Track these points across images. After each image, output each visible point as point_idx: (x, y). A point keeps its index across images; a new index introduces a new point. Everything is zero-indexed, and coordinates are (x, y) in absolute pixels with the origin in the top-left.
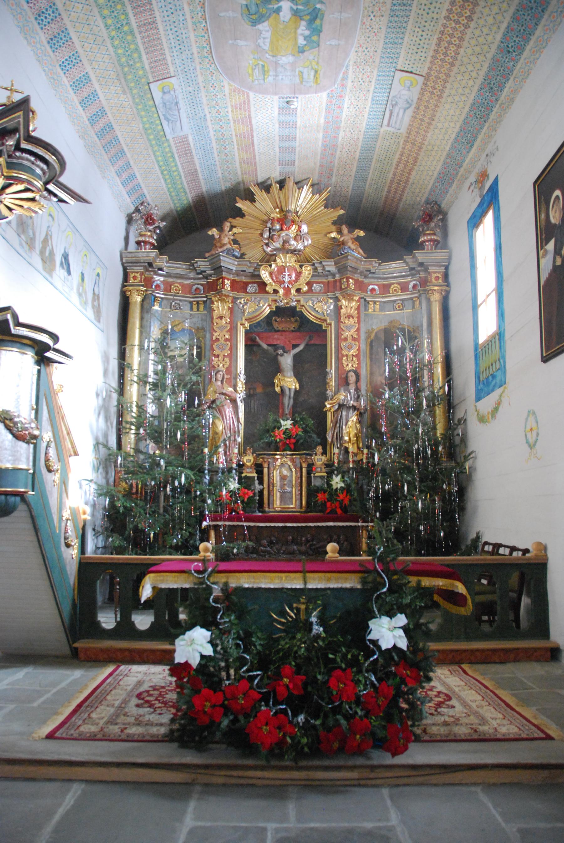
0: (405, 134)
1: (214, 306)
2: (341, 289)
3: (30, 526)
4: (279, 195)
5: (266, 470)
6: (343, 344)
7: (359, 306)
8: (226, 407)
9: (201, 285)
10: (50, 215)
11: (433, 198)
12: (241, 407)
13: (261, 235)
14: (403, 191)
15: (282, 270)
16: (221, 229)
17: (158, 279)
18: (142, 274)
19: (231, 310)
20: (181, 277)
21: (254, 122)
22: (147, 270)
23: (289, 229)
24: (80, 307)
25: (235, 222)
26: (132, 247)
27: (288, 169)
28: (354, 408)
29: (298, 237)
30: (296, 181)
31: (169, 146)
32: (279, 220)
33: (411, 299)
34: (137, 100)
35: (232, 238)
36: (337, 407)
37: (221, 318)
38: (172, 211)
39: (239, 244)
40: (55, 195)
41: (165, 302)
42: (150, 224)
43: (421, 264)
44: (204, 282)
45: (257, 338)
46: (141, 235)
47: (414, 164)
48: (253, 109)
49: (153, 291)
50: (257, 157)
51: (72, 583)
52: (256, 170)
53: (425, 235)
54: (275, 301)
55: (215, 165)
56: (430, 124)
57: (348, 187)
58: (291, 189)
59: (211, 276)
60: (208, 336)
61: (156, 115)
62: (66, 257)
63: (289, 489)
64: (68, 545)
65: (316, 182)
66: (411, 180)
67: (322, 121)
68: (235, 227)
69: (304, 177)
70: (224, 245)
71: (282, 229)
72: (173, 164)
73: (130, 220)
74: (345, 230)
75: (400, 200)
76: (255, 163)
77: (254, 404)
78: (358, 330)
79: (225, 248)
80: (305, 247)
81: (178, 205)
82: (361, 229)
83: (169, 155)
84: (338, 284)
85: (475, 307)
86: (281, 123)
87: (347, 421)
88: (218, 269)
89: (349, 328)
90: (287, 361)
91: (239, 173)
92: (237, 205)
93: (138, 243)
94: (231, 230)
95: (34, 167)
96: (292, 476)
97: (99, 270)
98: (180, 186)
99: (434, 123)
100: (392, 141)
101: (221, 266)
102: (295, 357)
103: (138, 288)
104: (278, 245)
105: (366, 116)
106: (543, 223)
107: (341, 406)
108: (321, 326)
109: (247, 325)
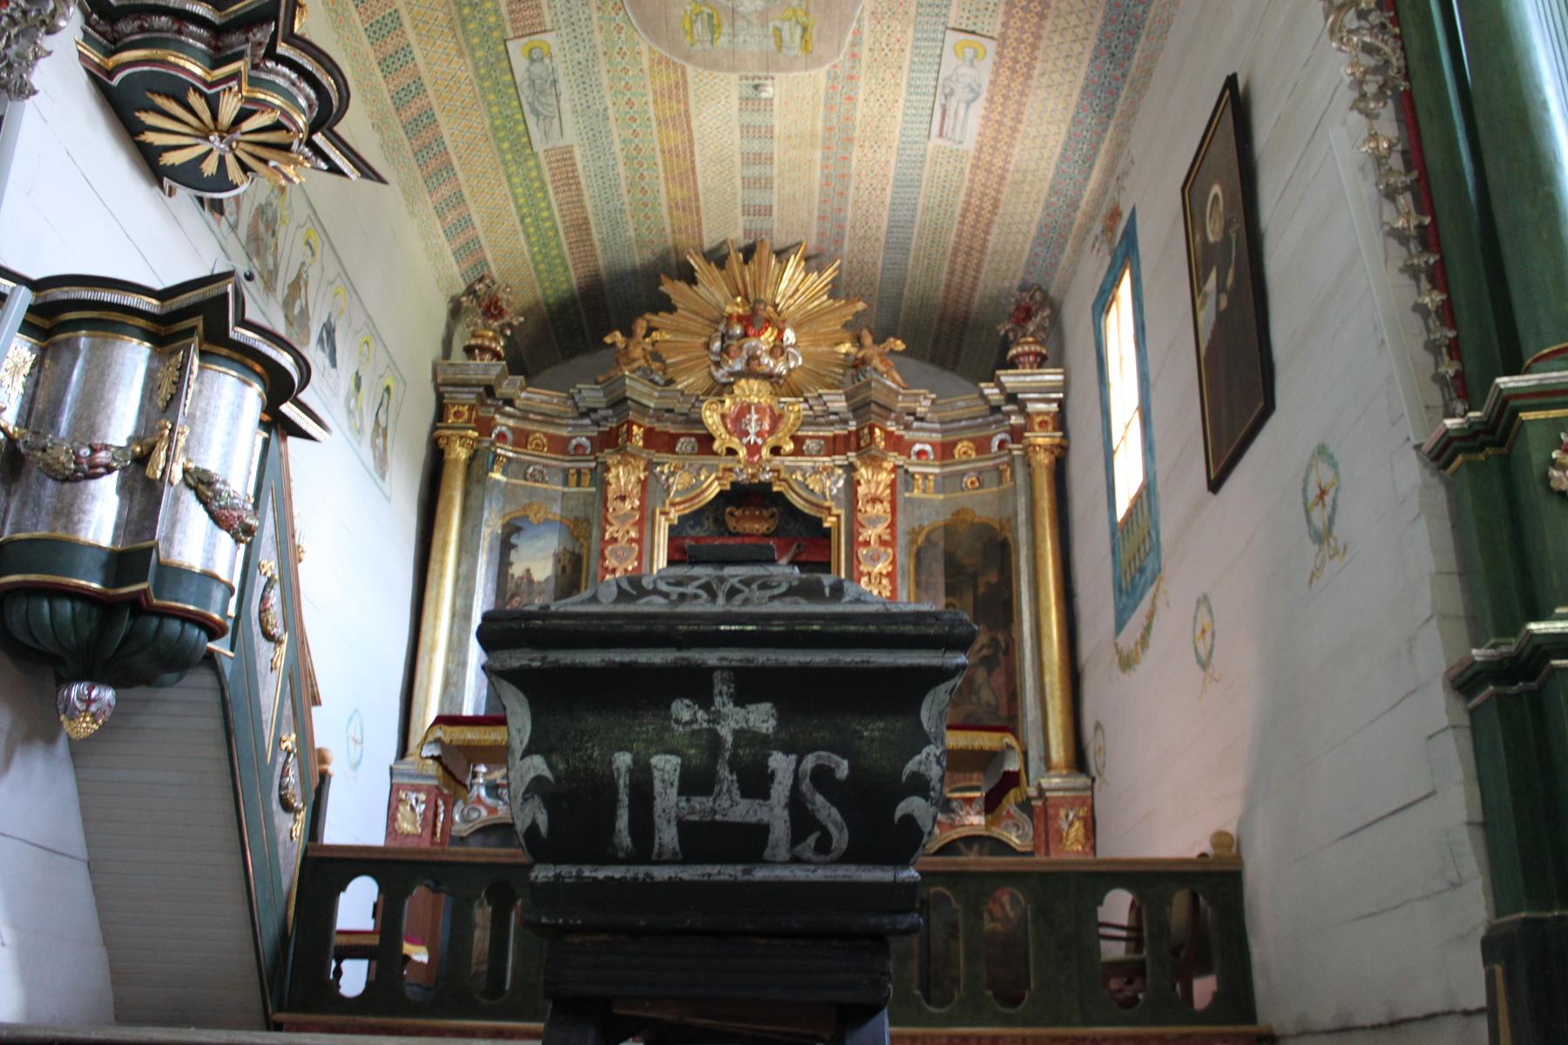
0: (972, 153)
1: (611, 477)
2: (858, 448)
3: (216, 724)
4: (742, 273)
6: (863, 552)
10: (308, 243)
11: (1033, 279)
13: (707, 346)
14: (979, 265)
16: (628, 333)
17: (503, 424)
18: (471, 408)
19: (643, 484)
21: (694, 124)
22: (483, 404)
23: (758, 335)
24: (348, 434)
25: (656, 319)
26: (458, 356)
27: (759, 223)
29: (778, 350)
30: (777, 247)
31: (538, 167)
32: (740, 319)
33: (996, 468)
34: (482, 71)
35: (649, 348)
37: (623, 498)
38: (537, 303)
39: (663, 362)
40: (326, 158)
41: (513, 466)
42: (495, 317)
43: (1011, 398)
46: (474, 335)
47: (993, 213)
48: (692, 99)
49: (493, 443)
50: (701, 197)
51: (285, 888)
52: (700, 224)
55: (622, 211)
56: (1014, 130)
57: (874, 264)
59: (606, 419)
60: (595, 533)
61: (515, 103)
62: (329, 331)
64: (287, 806)
65: (813, 252)
66: (990, 245)
67: (820, 126)
68: (656, 329)
69: (791, 241)
70: (634, 360)
71: (745, 335)
72: (543, 205)
73: (456, 311)
74: (868, 340)
75: (973, 289)
76: (698, 209)
78: (892, 526)
79: (636, 365)
80: (790, 370)
81: (549, 292)
82: (897, 337)
83: (537, 185)
84: (853, 439)
86: (745, 128)
88: (619, 403)
89: (874, 521)
91: (668, 230)
93: (469, 350)
94: (648, 334)
95: (294, 90)
97: (389, 381)
98: (554, 252)
99: (1021, 127)
100: (950, 168)
101: (626, 399)
103: (463, 433)
104: (739, 366)
105: (899, 116)
106: (1199, 248)
108: (820, 521)
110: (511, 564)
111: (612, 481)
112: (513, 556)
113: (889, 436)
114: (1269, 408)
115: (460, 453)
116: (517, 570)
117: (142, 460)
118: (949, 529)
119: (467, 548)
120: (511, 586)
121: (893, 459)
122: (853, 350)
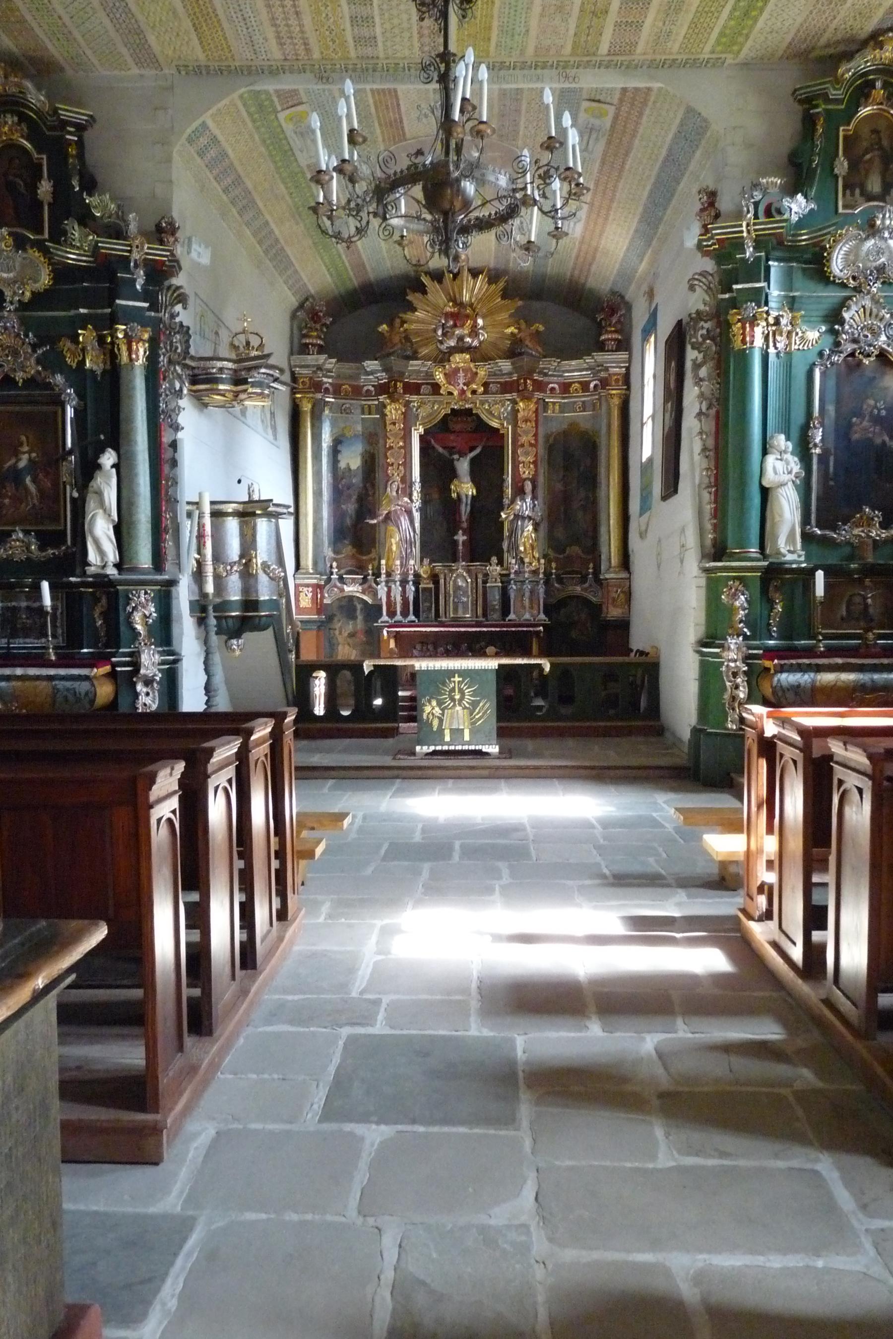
1: (387, 411)
2: (519, 391)
5: (442, 581)
7: (537, 409)
8: (402, 519)
9: (373, 386)
12: (417, 516)
13: (435, 331)
15: (457, 370)
28: (530, 518)
36: (512, 517)
37: (394, 424)
39: (411, 342)
45: (433, 441)
53: (608, 332)
55: (384, 259)
58: (465, 278)
60: (381, 441)
63: (465, 599)
68: (406, 322)
71: (455, 326)
74: (523, 326)
77: (430, 510)
78: (536, 435)
80: (481, 343)
85: (642, 425)
87: (523, 531)
89: (526, 433)
90: (463, 466)
92: (407, 298)
94: (402, 326)
96: (467, 586)
104: (452, 343)
107: (517, 517)
109: (421, 430)
110: (338, 461)
111: (388, 413)
112: (340, 457)
114: (676, 491)
115: (306, 407)
116: (342, 465)
117: (248, 565)
118: (565, 434)
120: (340, 473)
121: (538, 395)
122: (516, 331)
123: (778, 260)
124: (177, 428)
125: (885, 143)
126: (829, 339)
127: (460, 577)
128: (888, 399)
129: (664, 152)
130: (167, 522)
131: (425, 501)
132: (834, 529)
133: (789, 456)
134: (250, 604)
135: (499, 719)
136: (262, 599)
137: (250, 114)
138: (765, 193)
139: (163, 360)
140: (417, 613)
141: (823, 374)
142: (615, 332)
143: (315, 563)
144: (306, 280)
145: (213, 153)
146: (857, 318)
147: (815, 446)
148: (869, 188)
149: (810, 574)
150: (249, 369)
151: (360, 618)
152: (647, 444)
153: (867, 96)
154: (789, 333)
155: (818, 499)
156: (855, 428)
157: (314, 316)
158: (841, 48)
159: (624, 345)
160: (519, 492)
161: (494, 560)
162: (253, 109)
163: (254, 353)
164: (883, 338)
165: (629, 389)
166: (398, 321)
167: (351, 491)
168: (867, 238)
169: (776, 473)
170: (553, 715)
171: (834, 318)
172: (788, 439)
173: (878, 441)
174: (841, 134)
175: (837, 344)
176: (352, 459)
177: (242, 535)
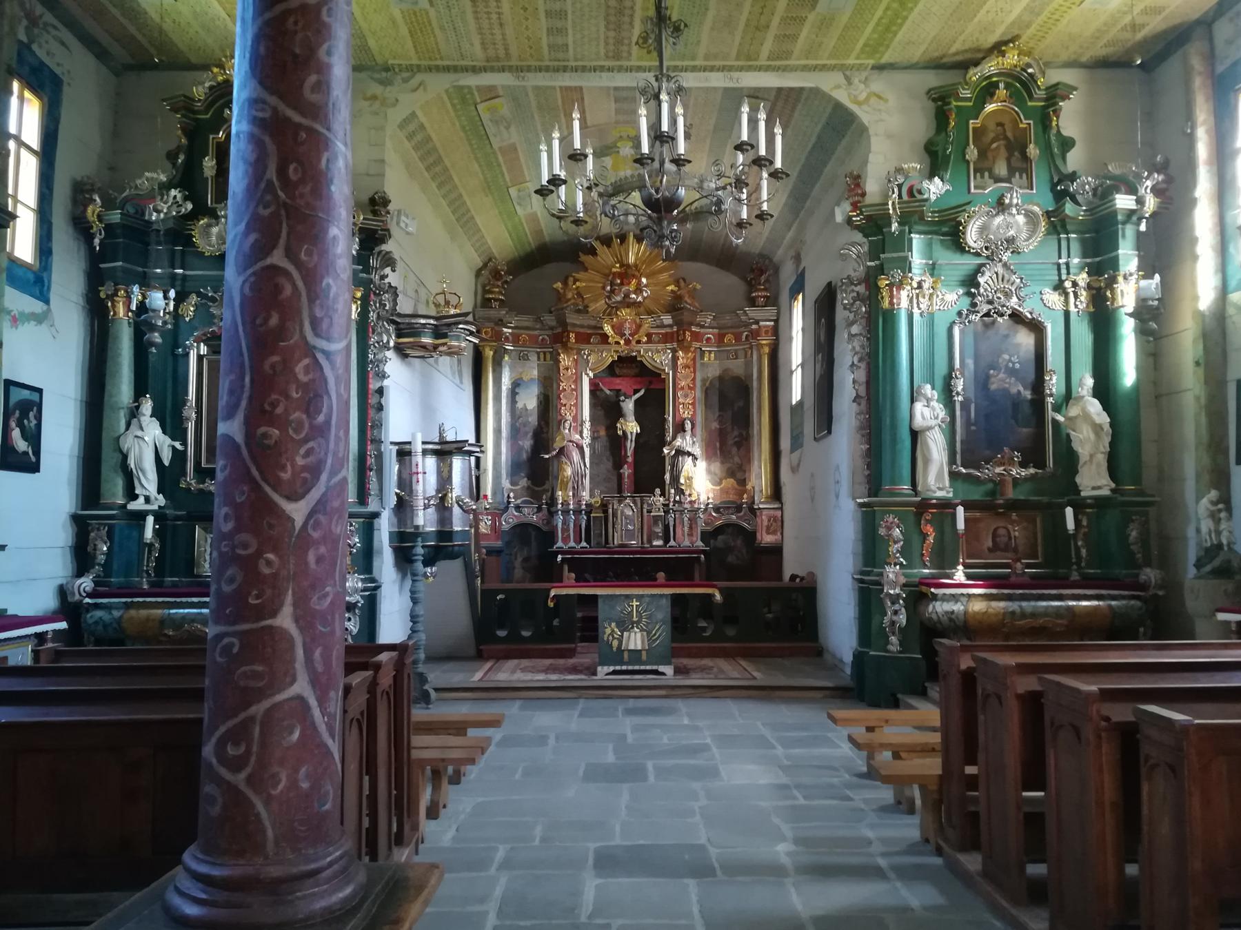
12: (587, 451)
13: (604, 288)
19: (576, 361)
20: (527, 328)
44: (550, 332)
54: (617, 352)
71: (622, 284)
74: (682, 284)
77: (598, 446)
78: (694, 380)
80: (645, 298)
88: (563, 323)
90: (629, 406)
102: (636, 401)
104: (619, 298)
109: (591, 374)
112: (517, 398)
113: (693, 333)
115: (489, 353)
116: (520, 405)
117: (443, 499)
119: (497, 398)
121: (696, 345)
122: (676, 289)
123: (920, 233)
124: (383, 376)
125: (1009, 134)
126: (967, 301)
127: (627, 509)
128: (1021, 354)
129: (814, 139)
130: (371, 461)
131: (594, 438)
132: (978, 468)
133: (934, 404)
134: (445, 534)
135: (673, 640)
136: (456, 529)
137: (453, 105)
138: (907, 177)
139: (373, 316)
140: (588, 541)
141: (962, 332)
142: (765, 290)
143: (494, 493)
144: (489, 242)
145: (419, 137)
146: (990, 282)
147: (958, 394)
148: (997, 171)
149: (954, 506)
150: (449, 325)
151: (534, 544)
152: (796, 389)
153: (992, 95)
154: (931, 295)
155: (962, 442)
156: (993, 380)
157: (496, 274)
158: (968, 56)
159: (773, 301)
160: (680, 428)
161: (658, 491)
162: (456, 101)
163: (452, 312)
164: (1015, 299)
165: (777, 339)
166: (571, 279)
167: (527, 429)
168: (997, 214)
169: (923, 418)
170: (718, 636)
171: (970, 282)
172: (933, 388)
173: (1014, 390)
174: (971, 126)
175: (974, 305)
176: (529, 401)
177: (439, 472)
